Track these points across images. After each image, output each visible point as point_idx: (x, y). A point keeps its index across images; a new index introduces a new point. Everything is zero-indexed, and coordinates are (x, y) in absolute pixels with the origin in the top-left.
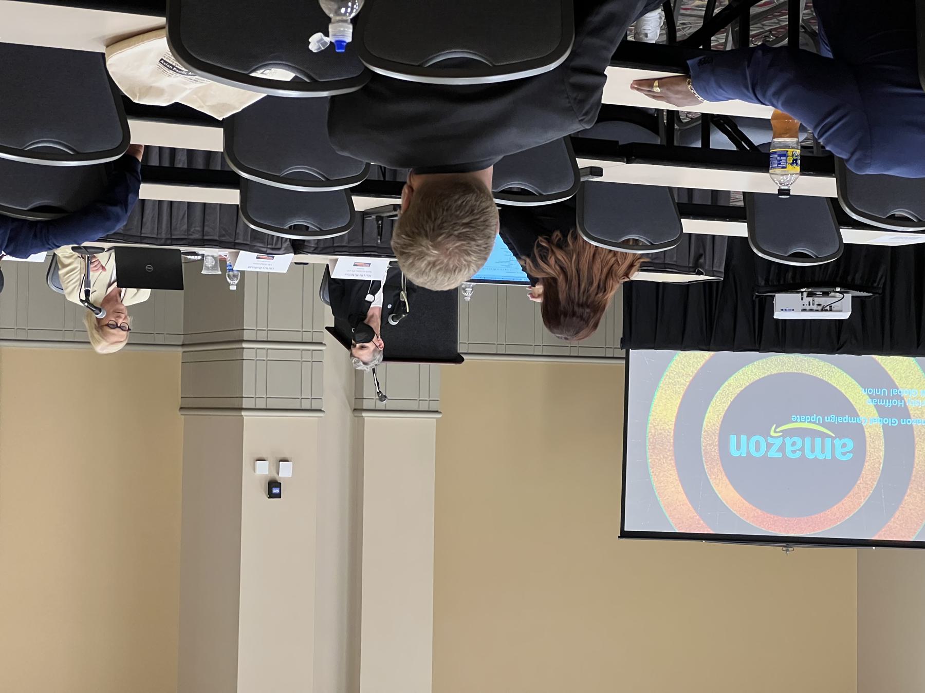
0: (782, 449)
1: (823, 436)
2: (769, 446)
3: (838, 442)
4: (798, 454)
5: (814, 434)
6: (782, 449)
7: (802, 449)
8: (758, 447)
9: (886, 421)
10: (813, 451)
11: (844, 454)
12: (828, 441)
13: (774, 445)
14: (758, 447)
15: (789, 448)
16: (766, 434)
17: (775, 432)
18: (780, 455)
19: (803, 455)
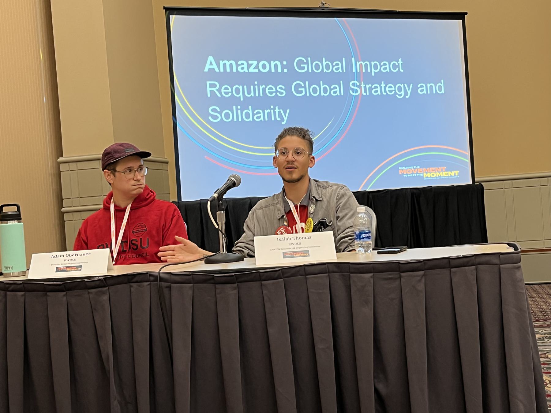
0: (249, 66)
2: (257, 67)
4: (240, 63)
6: (249, 66)
7: (237, 66)
9: (317, 66)
10: (231, 65)
13: (253, 68)
15: (245, 66)
18: (250, 62)
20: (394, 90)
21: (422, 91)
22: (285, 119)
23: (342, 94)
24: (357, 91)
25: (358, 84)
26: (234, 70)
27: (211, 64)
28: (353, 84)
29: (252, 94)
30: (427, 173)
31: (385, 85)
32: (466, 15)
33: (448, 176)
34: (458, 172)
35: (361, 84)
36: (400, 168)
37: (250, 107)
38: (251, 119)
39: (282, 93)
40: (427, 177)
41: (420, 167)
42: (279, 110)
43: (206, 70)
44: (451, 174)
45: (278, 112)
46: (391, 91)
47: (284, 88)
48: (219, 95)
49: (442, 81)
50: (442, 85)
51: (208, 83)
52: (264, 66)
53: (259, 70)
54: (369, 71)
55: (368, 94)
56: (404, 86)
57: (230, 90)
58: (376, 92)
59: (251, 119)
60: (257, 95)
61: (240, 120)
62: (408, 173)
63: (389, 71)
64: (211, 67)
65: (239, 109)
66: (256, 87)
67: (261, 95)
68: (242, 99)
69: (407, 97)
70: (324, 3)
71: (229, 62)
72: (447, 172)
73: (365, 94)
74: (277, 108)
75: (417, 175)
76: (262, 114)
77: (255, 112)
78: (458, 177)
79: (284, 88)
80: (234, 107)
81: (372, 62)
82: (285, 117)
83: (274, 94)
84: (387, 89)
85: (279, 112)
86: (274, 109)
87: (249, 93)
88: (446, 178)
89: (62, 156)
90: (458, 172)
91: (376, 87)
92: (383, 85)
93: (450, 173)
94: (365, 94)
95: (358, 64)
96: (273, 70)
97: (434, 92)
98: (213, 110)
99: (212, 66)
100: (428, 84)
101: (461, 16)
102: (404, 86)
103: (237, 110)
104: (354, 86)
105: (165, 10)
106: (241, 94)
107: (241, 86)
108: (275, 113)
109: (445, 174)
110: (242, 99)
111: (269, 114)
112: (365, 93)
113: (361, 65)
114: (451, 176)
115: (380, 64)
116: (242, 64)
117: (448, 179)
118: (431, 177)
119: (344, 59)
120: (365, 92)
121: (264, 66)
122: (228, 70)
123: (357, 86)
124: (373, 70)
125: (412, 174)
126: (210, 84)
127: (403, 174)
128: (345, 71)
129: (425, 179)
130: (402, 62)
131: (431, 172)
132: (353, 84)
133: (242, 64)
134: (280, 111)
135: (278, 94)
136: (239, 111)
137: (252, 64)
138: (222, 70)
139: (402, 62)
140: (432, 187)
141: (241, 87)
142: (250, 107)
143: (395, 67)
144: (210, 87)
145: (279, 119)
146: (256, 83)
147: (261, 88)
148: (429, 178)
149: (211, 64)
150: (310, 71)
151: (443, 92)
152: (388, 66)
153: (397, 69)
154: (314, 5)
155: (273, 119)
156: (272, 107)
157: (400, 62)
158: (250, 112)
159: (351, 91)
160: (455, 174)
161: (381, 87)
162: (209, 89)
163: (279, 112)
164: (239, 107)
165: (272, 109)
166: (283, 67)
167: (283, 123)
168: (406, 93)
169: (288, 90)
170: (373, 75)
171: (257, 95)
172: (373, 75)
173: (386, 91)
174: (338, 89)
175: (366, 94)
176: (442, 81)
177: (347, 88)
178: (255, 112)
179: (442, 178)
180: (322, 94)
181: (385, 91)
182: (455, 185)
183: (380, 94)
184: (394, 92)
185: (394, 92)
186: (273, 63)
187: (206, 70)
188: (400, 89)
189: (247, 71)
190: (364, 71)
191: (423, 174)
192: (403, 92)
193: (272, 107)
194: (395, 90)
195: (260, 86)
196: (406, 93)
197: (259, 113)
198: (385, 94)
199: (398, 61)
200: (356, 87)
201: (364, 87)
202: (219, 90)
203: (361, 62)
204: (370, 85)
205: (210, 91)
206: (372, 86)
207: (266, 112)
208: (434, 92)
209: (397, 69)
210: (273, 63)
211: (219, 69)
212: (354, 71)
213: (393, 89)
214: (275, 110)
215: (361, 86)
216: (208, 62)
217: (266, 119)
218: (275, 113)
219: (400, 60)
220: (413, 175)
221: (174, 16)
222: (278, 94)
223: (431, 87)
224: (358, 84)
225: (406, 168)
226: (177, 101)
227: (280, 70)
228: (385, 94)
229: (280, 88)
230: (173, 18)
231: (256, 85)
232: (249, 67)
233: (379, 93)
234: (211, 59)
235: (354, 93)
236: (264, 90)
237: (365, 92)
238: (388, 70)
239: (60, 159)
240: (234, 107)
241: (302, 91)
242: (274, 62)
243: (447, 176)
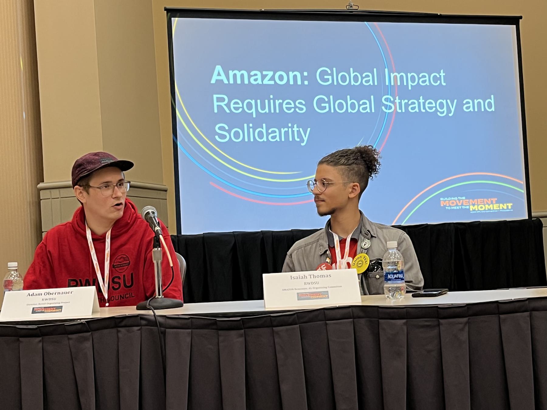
0: (264, 77)
2: (273, 78)
4: (252, 73)
6: (264, 77)
7: (250, 77)
10: (242, 76)
15: (259, 76)
18: (264, 73)
20: (434, 107)
21: (468, 108)
22: (306, 139)
23: (373, 111)
24: (390, 108)
25: (392, 99)
26: (246, 82)
27: (219, 74)
28: (387, 100)
29: (267, 110)
30: (474, 205)
31: (424, 101)
32: (520, 20)
33: (500, 210)
34: (512, 204)
35: (396, 100)
36: (442, 199)
37: (264, 125)
38: (265, 139)
39: (301, 109)
40: (474, 210)
41: (466, 198)
42: (298, 129)
43: (213, 81)
44: (502, 207)
45: (297, 130)
46: (431, 108)
47: (304, 103)
48: (228, 111)
49: (492, 96)
50: (492, 102)
51: (215, 96)
52: (281, 78)
53: (275, 82)
54: (405, 84)
55: (404, 111)
56: (447, 102)
57: (241, 105)
58: (413, 108)
59: (265, 139)
60: (272, 111)
61: (252, 140)
62: (451, 205)
63: (428, 84)
64: (219, 78)
65: (251, 127)
66: (272, 101)
67: (278, 111)
68: (254, 116)
69: (450, 115)
70: (352, 4)
71: (239, 72)
72: (498, 205)
73: (400, 111)
74: (295, 126)
75: (462, 208)
76: (277, 134)
77: (270, 131)
78: (512, 210)
79: (304, 103)
80: (245, 125)
81: (409, 74)
82: (305, 137)
83: (293, 110)
84: (427, 105)
85: (299, 132)
86: (292, 127)
87: (263, 108)
88: (497, 211)
89: (43, 181)
90: (512, 204)
91: (413, 103)
92: (421, 101)
93: (501, 205)
94: (400, 111)
95: (392, 75)
96: (292, 82)
97: (483, 110)
98: (221, 128)
99: (220, 77)
100: (475, 100)
101: (514, 21)
102: (447, 102)
103: (249, 128)
104: (388, 102)
105: (166, 12)
106: (254, 110)
107: (254, 101)
108: (293, 132)
109: (496, 207)
110: (254, 116)
111: (287, 133)
112: (400, 109)
113: (395, 77)
114: (503, 209)
115: (418, 76)
116: (256, 75)
117: (499, 213)
118: (479, 210)
119: (375, 70)
120: (401, 108)
121: (281, 78)
122: (239, 81)
123: (391, 102)
124: (410, 83)
125: (457, 205)
126: (217, 98)
127: (445, 206)
128: (376, 84)
129: (471, 212)
130: (444, 74)
131: (479, 204)
132: (387, 100)
133: (256, 75)
134: (299, 130)
135: (297, 110)
136: (251, 130)
137: (267, 75)
138: (232, 81)
139: (444, 74)
140: (480, 221)
141: (253, 102)
142: (264, 125)
143: (436, 79)
144: (217, 102)
145: (298, 140)
146: (271, 97)
147: (277, 102)
148: (476, 211)
149: (219, 74)
150: (335, 83)
151: (493, 109)
152: (427, 78)
153: (439, 82)
154: (341, 6)
155: (291, 139)
156: (290, 125)
157: (442, 74)
158: (264, 131)
159: (383, 108)
160: (507, 207)
161: (419, 103)
162: (216, 104)
163: (299, 132)
164: (251, 125)
165: (290, 127)
166: (303, 78)
167: (303, 144)
168: (449, 111)
169: (309, 105)
170: (410, 88)
171: (272, 111)
172: (410, 88)
173: (425, 108)
174: (368, 105)
175: (402, 111)
176: (492, 96)
177: (378, 103)
178: (270, 131)
179: (491, 211)
180: (350, 110)
181: (424, 108)
182: (507, 220)
183: (418, 111)
184: (434, 109)
185: (434, 109)
186: (291, 74)
187: (213, 81)
188: (442, 106)
189: (260, 83)
190: (399, 84)
191: (469, 207)
192: (445, 109)
193: (290, 125)
194: (436, 107)
195: (277, 101)
196: (449, 111)
197: (275, 132)
198: (424, 111)
199: (439, 73)
200: (390, 102)
201: (399, 102)
202: (228, 105)
203: (396, 74)
204: (406, 101)
205: (217, 105)
206: (408, 102)
207: (283, 131)
208: (483, 110)
209: (439, 82)
210: (291, 74)
211: (228, 79)
212: (387, 84)
213: (434, 105)
214: (293, 129)
215: (396, 101)
216: (216, 73)
217: (283, 140)
218: (293, 132)
219: (442, 71)
220: (458, 208)
221: (177, 19)
222: (297, 110)
223: (479, 103)
224: (392, 99)
225: (449, 199)
226: (178, 117)
227: (299, 82)
228: (424, 111)
229: (300, 103)
230: (175, 21)
231: (271, 99)
233: (417, 110)
234: (219, 68)
235: (387, 109)
236: (281, 105)
237: (401, 108)
238: (427, 83)
239: (41, 185)
240: (245, 125)
241: (326, 106)
242: (293, 73)
243: (499, 209)
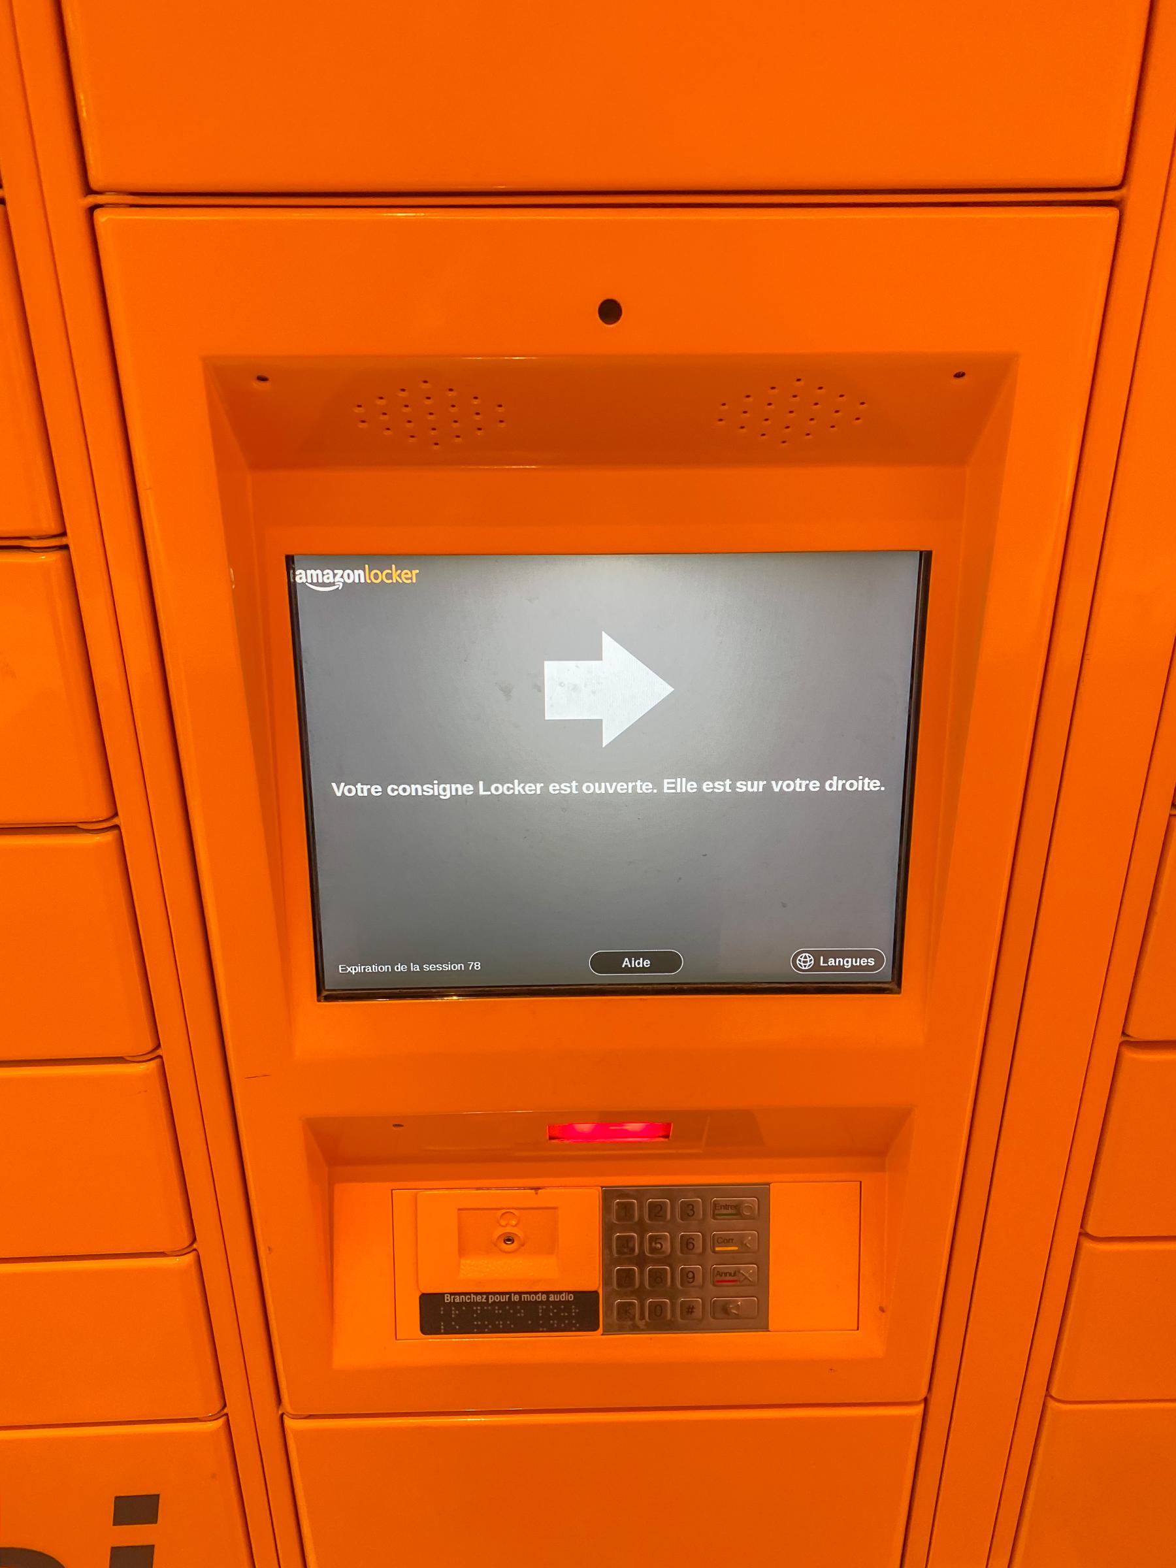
0: (335, 575)
1: (312, 583)
2: (342, 577)
3: (305, 581)
4: (325, 572)
5: (318, 584)
6: (335, 575)
7: (323, 575)
8: (348, 574)
11: (300, 574)
12: (310, 581)
14: (348, 574)
16: (344, 583)
17: (339, 585)
18: (336, 571)
19: (323, 572)
96: (357, 581)
122: (315, 581)
137: (337, 574)
232: (334, 577)
